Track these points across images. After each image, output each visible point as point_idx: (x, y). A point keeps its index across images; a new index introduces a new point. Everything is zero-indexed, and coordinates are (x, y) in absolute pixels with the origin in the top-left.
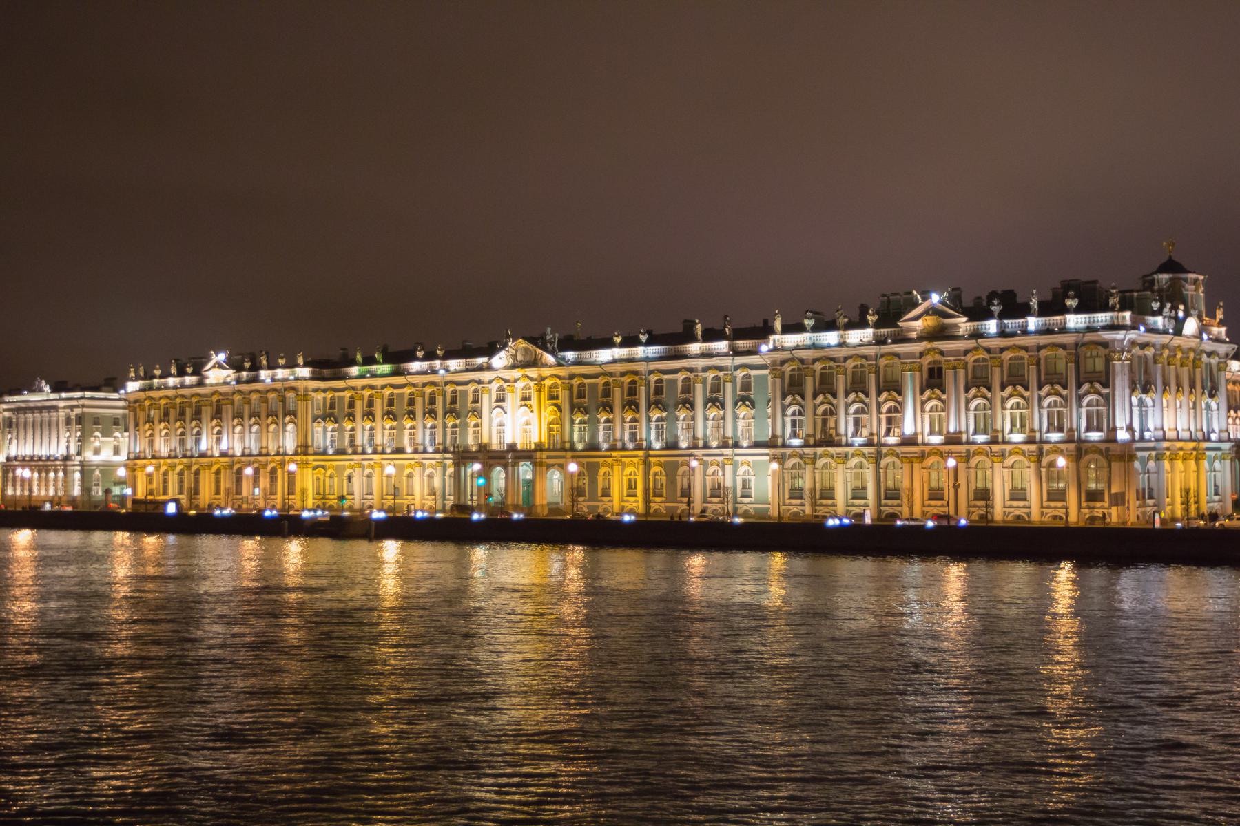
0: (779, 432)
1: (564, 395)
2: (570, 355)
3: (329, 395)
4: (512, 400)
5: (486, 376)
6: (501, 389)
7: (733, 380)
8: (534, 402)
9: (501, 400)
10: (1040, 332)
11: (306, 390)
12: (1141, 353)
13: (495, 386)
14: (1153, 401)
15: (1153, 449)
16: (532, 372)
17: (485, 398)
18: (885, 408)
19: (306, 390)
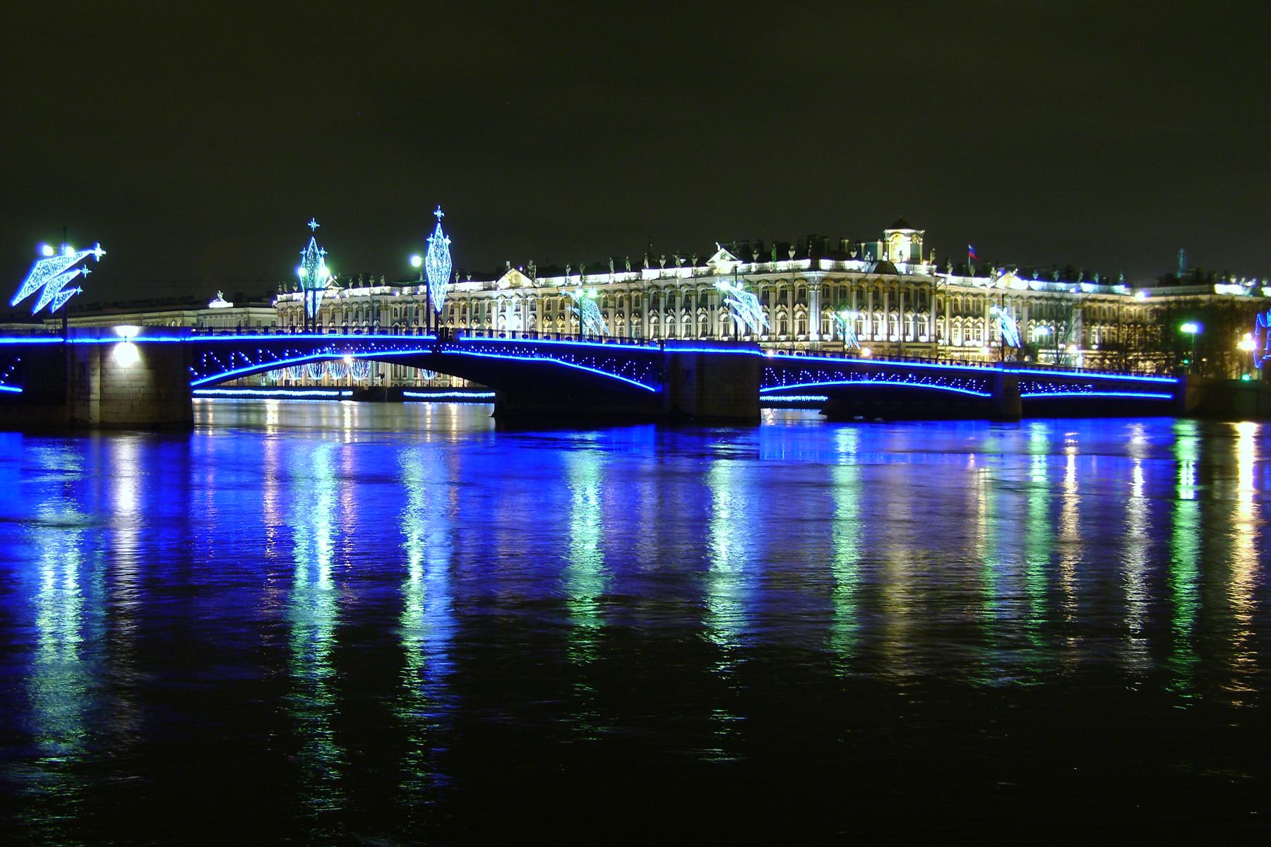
0: (646, 334)
1: (539, 308)
2: (542, 281)
3: (404, 306)
4: (510, 311)
5: (494, 294)
6: (503, 303)
7: (630, 299)
8: (521, 312)
9: (504, 311)
10: (758, 272)
11: (386, 302)
12: (837, 285)
13: (500, 301)
16: (520, 292)
17: (494, 309)
18: (701, 318)
19: (386, 302)
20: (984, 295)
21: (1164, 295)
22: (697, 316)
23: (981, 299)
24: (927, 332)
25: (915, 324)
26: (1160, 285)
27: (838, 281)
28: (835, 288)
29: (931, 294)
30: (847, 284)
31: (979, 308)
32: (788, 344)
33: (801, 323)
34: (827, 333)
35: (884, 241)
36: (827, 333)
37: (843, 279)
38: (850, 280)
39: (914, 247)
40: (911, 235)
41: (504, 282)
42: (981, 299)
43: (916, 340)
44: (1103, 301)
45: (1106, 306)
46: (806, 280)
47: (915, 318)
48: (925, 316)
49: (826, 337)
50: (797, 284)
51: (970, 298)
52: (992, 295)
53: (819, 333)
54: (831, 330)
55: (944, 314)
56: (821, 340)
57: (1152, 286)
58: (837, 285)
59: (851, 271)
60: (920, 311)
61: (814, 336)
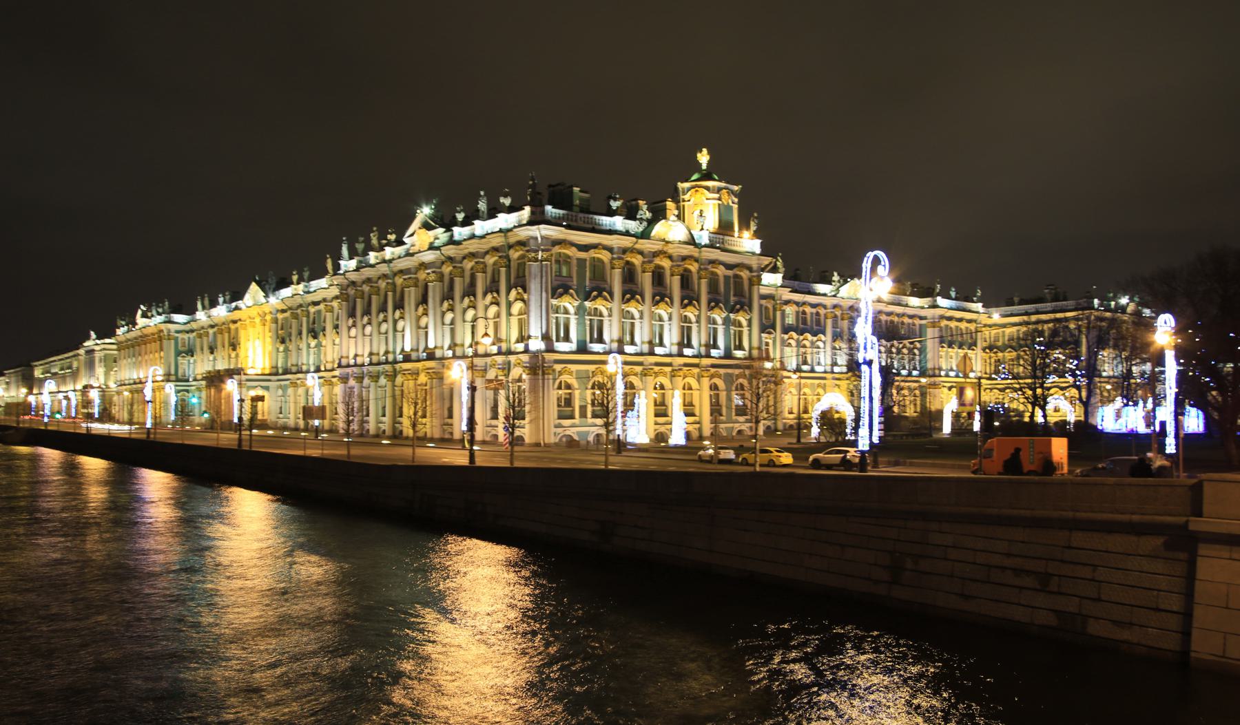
14: (610, 310)
15: (748, 367)
20: (825, 307)
21: (1027, 314)
22: (395, 322)
23: (822, 311)
24: (746, 344)
25: (727, 331)
26: (1023, 302)
27: (585, 248)
28: (581, 262)
29: (751, 284)
30: (605, 256)
31: (818, 323)
32: (500, 359)
33: (520, 322)
34: (567, 339)
35: (676, 201)
36: (567, 339)
37: (595, 246)
38: (610, 249)
39: (724, 211)
40: (719, 190)
41: (248, 299)
42: (822, 311)
43: (728, 355)
44: (960, 320)
45: (963, 325)
46: (522, 243)
47: (727, 322)
48: (742, 318)
49: (561, 346)
50: (515, 254)
51: (808, 310)
52: (835, 306)
53: (546, 337)
54: (573, 335)
55: (773, 327)
56: (550, 350)
57: (1010, 303)
58: (583, 255)
59: (611, 232)
60: (732, 310)
61: (536, 345)
